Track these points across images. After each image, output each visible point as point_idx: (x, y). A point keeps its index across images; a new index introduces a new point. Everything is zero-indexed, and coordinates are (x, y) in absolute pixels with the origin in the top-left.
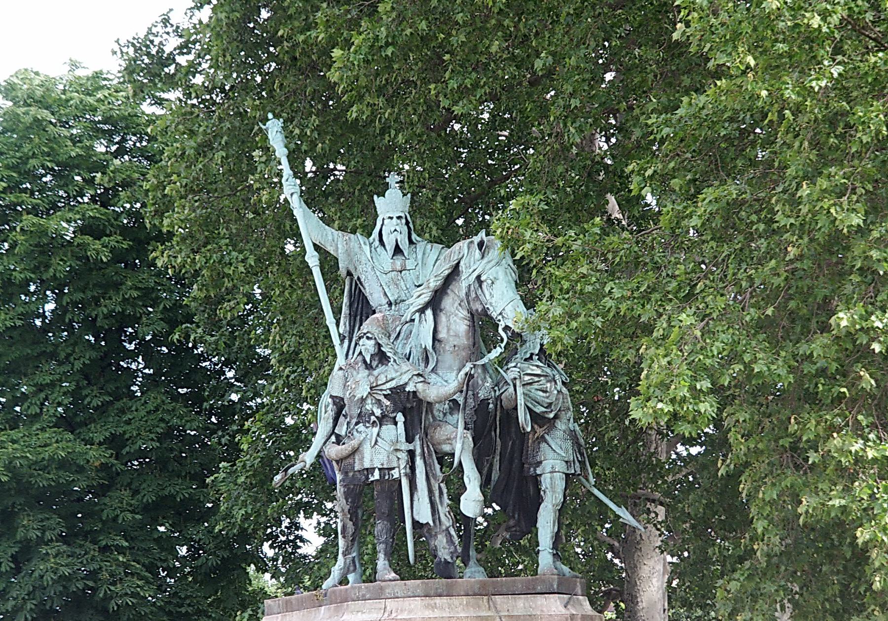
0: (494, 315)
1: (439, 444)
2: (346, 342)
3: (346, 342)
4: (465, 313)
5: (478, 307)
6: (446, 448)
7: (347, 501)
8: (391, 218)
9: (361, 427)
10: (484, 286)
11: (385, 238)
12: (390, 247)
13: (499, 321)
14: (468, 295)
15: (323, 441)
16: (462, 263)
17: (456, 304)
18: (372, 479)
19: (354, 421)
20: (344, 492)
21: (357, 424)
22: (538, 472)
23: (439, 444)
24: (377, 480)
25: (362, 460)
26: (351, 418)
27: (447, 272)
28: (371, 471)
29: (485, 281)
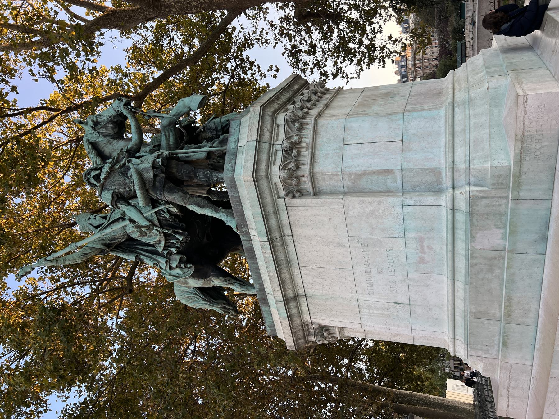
0: (114, 113)
1: (169, 145)
2: (141, 257)
3: (141, 257)
4: (115, 141)
5: (110, 129)
6: (172, 139)
7: (176, 192)
8: (89, 219)
9: (129, 173)
10: (99, 120)
11: (96, 223)
12: (103, 221)
13: (118, 111)
14: (105, 135)
15: (139, 214)
16: (91, 140)
17: (110, 146)
18: (160, 163)
19: (127, 181)
20: (169, 192)
21: (127, 177)
22: (220, 128)
23: (169, 145)
24: (162, 160)
25: (146, 169)
26: (126, 184)
27: (90, 146)
28: (154, 166)
29: (97, 119)
